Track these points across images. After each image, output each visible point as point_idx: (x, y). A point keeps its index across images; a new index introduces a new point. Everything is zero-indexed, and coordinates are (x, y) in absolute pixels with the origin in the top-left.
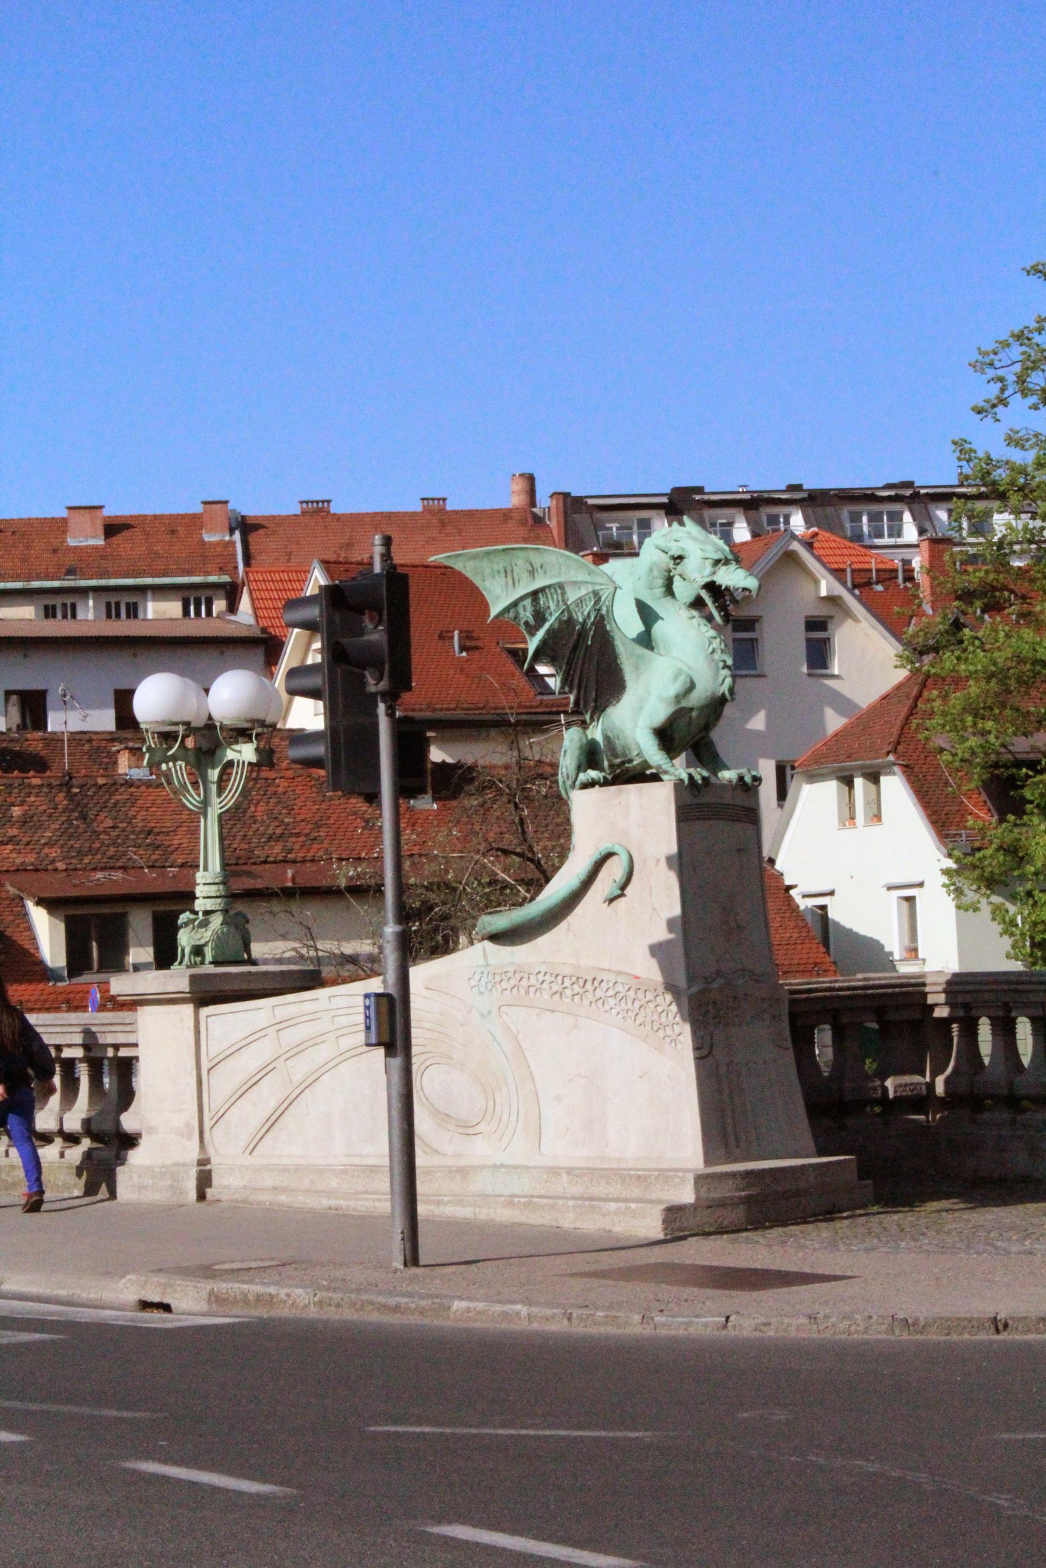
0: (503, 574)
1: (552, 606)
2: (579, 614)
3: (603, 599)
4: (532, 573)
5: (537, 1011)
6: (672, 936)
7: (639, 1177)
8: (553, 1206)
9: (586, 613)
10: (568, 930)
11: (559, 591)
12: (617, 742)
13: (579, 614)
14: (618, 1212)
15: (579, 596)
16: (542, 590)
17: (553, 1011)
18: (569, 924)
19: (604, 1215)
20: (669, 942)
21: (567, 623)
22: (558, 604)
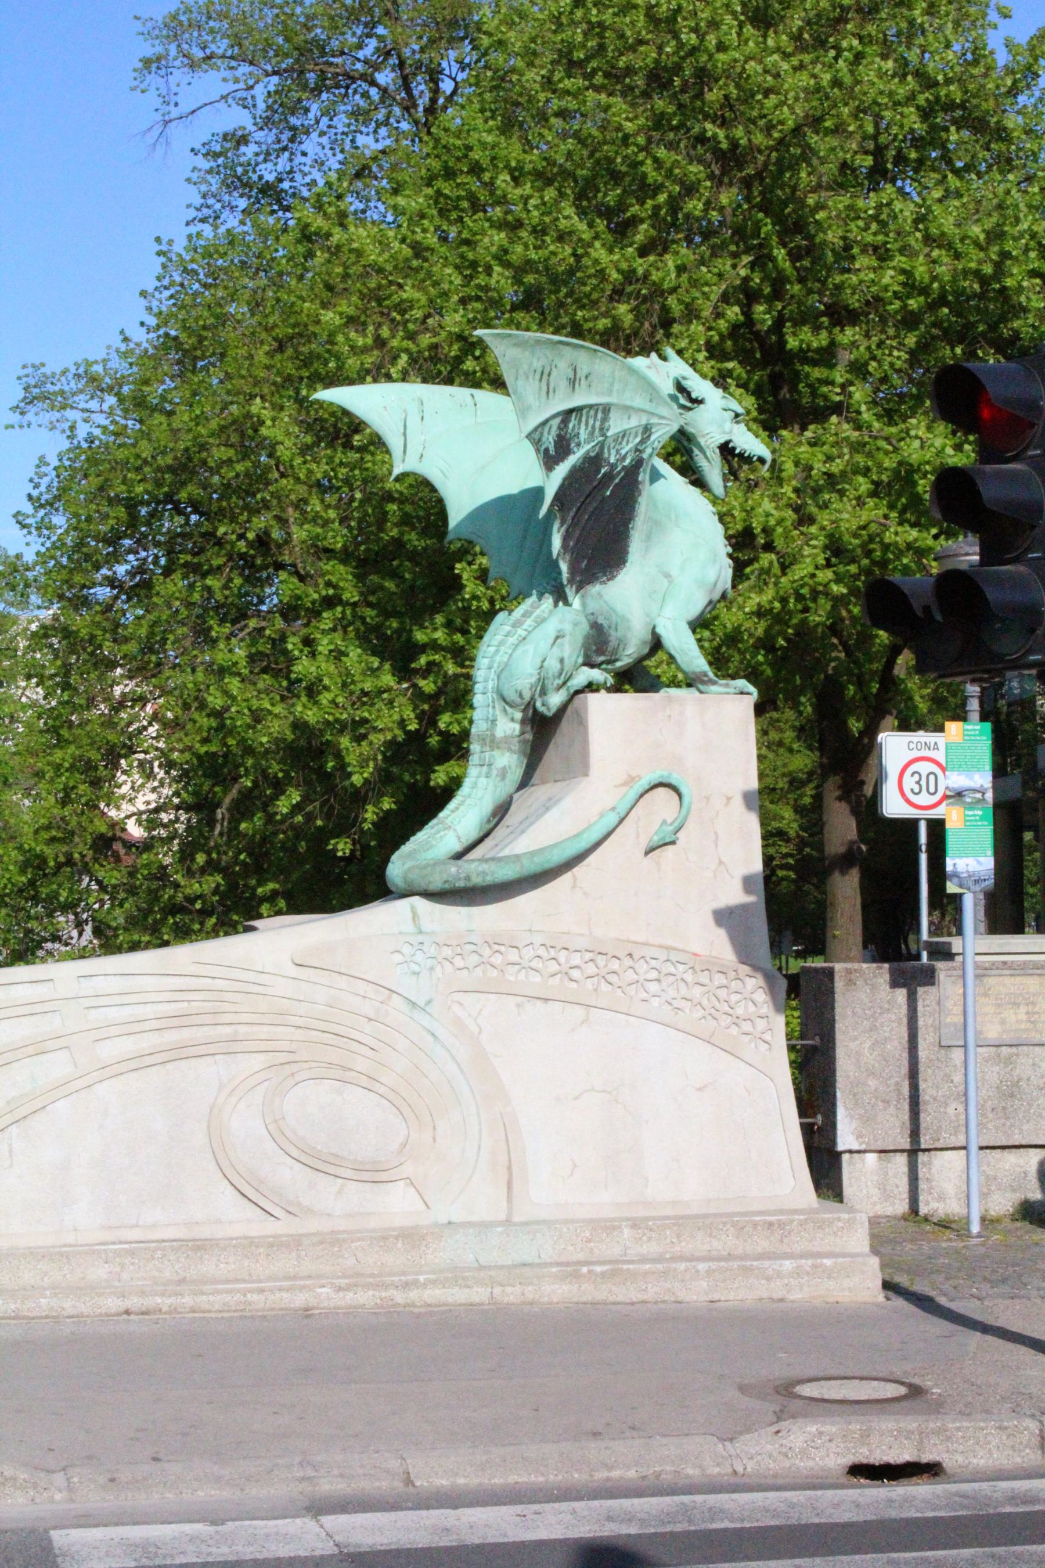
0: (538, 377)
1: (583, 435)
2: (613, 452)
3: (653, 438)
4: (573, 382)
5: (519, 999)
6: (751, 899)
7: (771, 1224)
8: (665, 1273)
9: (623, 452)
10: (574, 887)
11: (600, 415)
12: (612, 632)
13: (613, 452)
14: (797, 1273)
15: (626, 427)
16: (577, 410)
17: (546, 1000)
18: (575, 878)
19: (768, 1279)
20: (744, 907)
21: (593, 461)
22: (592, 433)
